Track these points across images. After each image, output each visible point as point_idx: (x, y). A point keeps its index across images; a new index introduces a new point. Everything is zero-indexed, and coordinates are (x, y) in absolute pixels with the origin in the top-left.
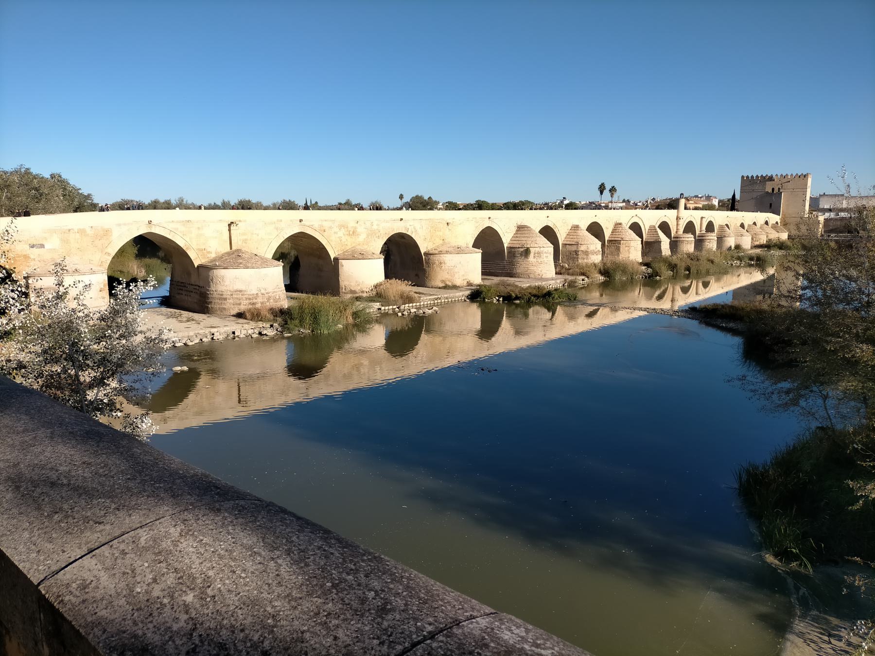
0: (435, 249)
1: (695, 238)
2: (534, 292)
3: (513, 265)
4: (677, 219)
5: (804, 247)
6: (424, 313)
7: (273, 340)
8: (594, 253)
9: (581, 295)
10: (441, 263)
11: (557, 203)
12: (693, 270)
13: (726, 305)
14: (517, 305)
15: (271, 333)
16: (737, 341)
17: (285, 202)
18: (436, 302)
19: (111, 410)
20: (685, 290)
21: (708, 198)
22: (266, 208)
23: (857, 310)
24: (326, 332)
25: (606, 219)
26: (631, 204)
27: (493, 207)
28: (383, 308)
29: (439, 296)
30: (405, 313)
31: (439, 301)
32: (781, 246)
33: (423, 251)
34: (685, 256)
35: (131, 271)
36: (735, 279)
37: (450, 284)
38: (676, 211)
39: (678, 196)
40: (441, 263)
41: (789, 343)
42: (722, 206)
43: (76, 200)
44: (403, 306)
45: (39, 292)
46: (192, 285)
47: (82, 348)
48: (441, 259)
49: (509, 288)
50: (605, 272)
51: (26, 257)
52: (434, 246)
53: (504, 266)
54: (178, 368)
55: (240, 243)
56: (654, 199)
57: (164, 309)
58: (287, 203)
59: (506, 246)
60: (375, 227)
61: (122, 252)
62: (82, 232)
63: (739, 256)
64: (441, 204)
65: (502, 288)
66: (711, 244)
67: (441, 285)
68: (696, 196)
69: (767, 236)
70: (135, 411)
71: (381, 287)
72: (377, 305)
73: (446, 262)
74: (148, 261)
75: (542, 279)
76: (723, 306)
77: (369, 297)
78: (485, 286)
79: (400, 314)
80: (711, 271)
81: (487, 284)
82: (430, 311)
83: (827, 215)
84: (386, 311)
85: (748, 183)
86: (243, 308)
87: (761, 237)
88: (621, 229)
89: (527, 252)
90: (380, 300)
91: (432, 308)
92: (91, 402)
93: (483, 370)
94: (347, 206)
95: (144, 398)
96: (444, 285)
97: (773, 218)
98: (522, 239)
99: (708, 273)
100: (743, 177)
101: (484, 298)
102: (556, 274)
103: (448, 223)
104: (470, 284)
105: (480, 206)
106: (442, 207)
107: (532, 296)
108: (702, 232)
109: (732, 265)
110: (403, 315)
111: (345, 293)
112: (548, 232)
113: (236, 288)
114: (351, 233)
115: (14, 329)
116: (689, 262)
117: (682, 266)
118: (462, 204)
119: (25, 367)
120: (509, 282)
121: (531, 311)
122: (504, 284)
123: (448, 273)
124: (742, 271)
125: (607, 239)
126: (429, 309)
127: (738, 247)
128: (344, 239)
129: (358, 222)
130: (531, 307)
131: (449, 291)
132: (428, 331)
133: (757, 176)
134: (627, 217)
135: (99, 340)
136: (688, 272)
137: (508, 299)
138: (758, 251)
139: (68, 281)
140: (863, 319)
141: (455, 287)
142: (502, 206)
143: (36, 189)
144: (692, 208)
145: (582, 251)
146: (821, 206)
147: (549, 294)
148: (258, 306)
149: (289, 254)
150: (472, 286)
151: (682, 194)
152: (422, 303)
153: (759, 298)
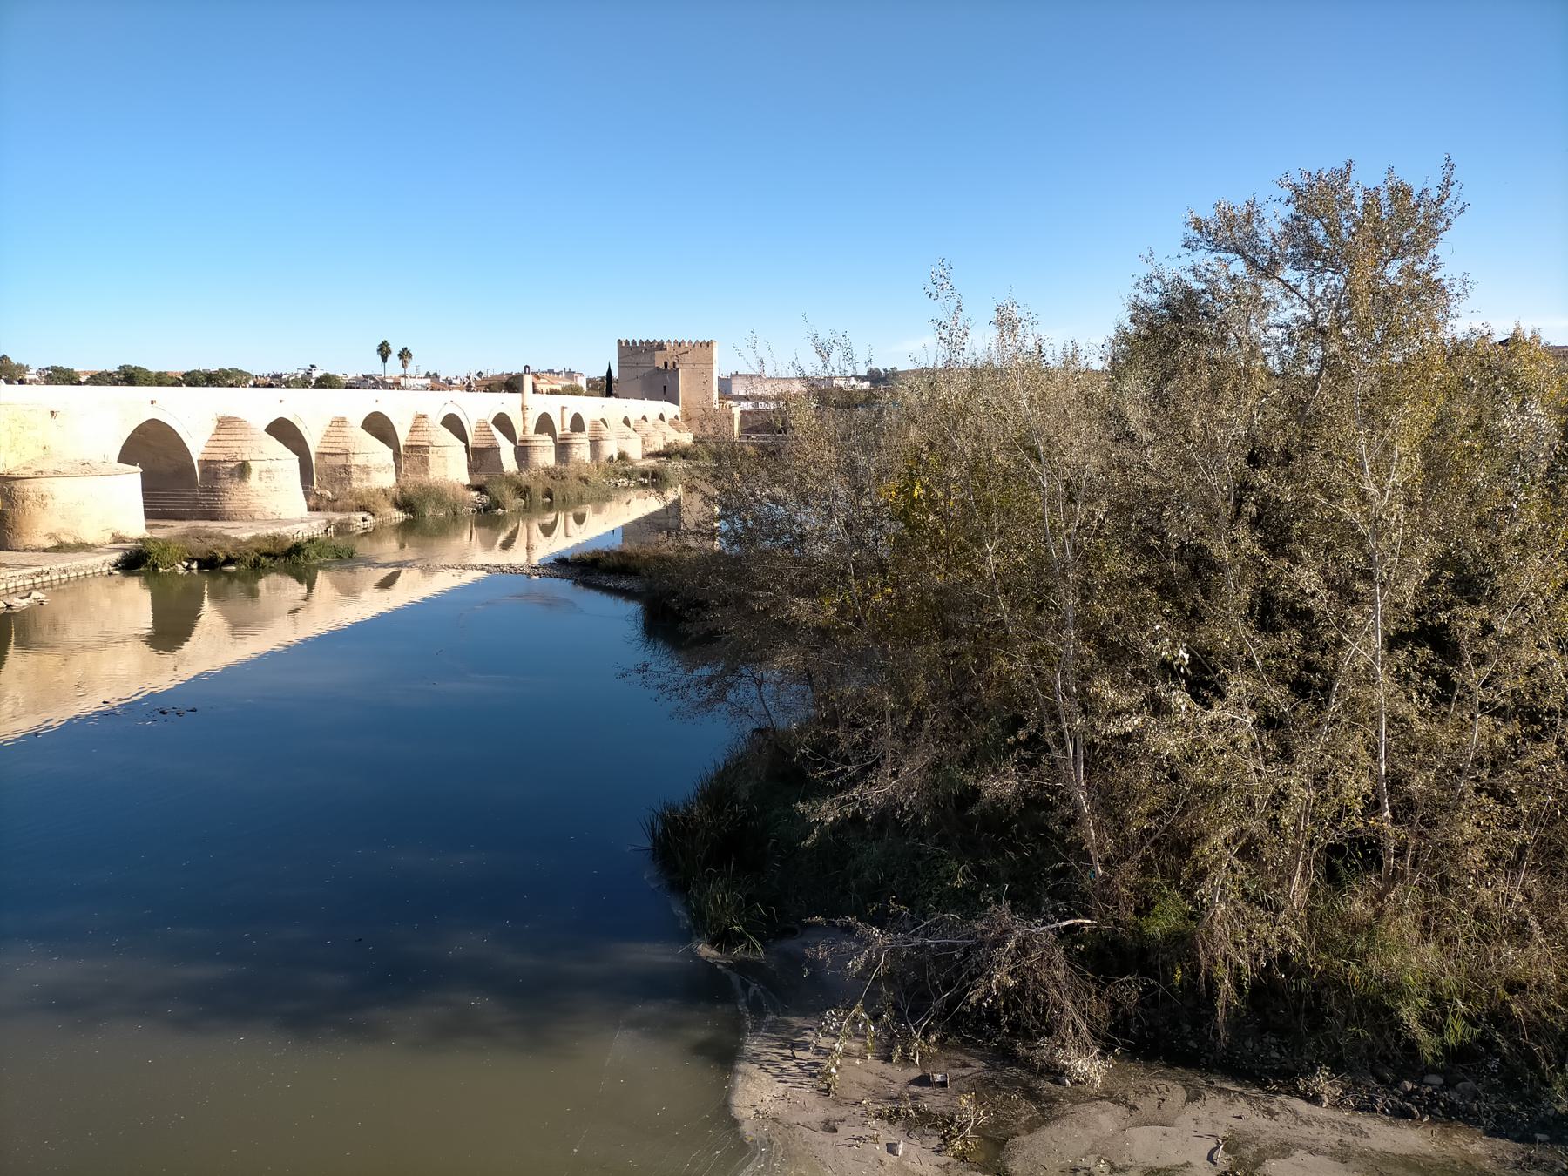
0: (25, 468)
1: (555, 441)
2: (266, 547)
3: (216, 496)
4: (522, 409)
5: (717, 457)
6: (9, 606)
8: (380, 469)
9: (363, 548)
11: (299, 376)
12: (557, 494)
13: (612, 551)
14: (231, 576)
16: (633, 608)
18: (38, 580)
20: (548, 530)
21: (570, 374)
25: (399, 408)
26: (441, 381)
27: (161, 380)
32: (684, 454)
34: (542, 471)
36: (623, 506)
37: (70, 540)
38: (519, 395)
39: (521, 370)
42: (592, 389)
49: (211, 543)
50: (404, 504)
53: (198, 500)
56: (480, 374)
59: (196, 457)
63: (625, 471)
65: (194, 543)
67: (48, 544)
68: (551, 372)
69: (665, 439)
75: (279, 521)
76: (607, 553)
78: (155, 541)
80: (586, 496)
81: (161, 536)
82: (25, 603)
83: (744, 404)
85: (630, 352)
87: (655, 439)
88: (426, 425)
89: (243, 470)
93: (163, 713)
96: (55, 544)
97: (671, 410)
98: (231, 444)
99: (581, 500)
100: (619, 342)
101: (155, 566)
102: (309, 510)
103: (52, 413)
104: (117, 539)
105: (130, 377)
106: (37, 378)
107: (261, 555)
108: (565, 432)
109: (617, 485)
112: (283, 431)
116: (549, 482)
117: (537, 489)
118: (86, 373)
120: (211, 530)
121: (262, 584)
122: (197, 535)
124: (632, 495)
125: (402, 443)
126: (21, 598)
127: (623, 456)
130: (261, 578)
132: (24, 644)
133: (641, 342)
134: (437, 405)
136: (548, 500)
137: (210, 564)
138: (653, 462)
141: (82, 547)
142: (181, 378)
144: (545, 391)
145: (357, 466)
146: (735, 392)
147: (297, 549)
150: (124, 542)
151: (527, 367)
153: (662, 536)
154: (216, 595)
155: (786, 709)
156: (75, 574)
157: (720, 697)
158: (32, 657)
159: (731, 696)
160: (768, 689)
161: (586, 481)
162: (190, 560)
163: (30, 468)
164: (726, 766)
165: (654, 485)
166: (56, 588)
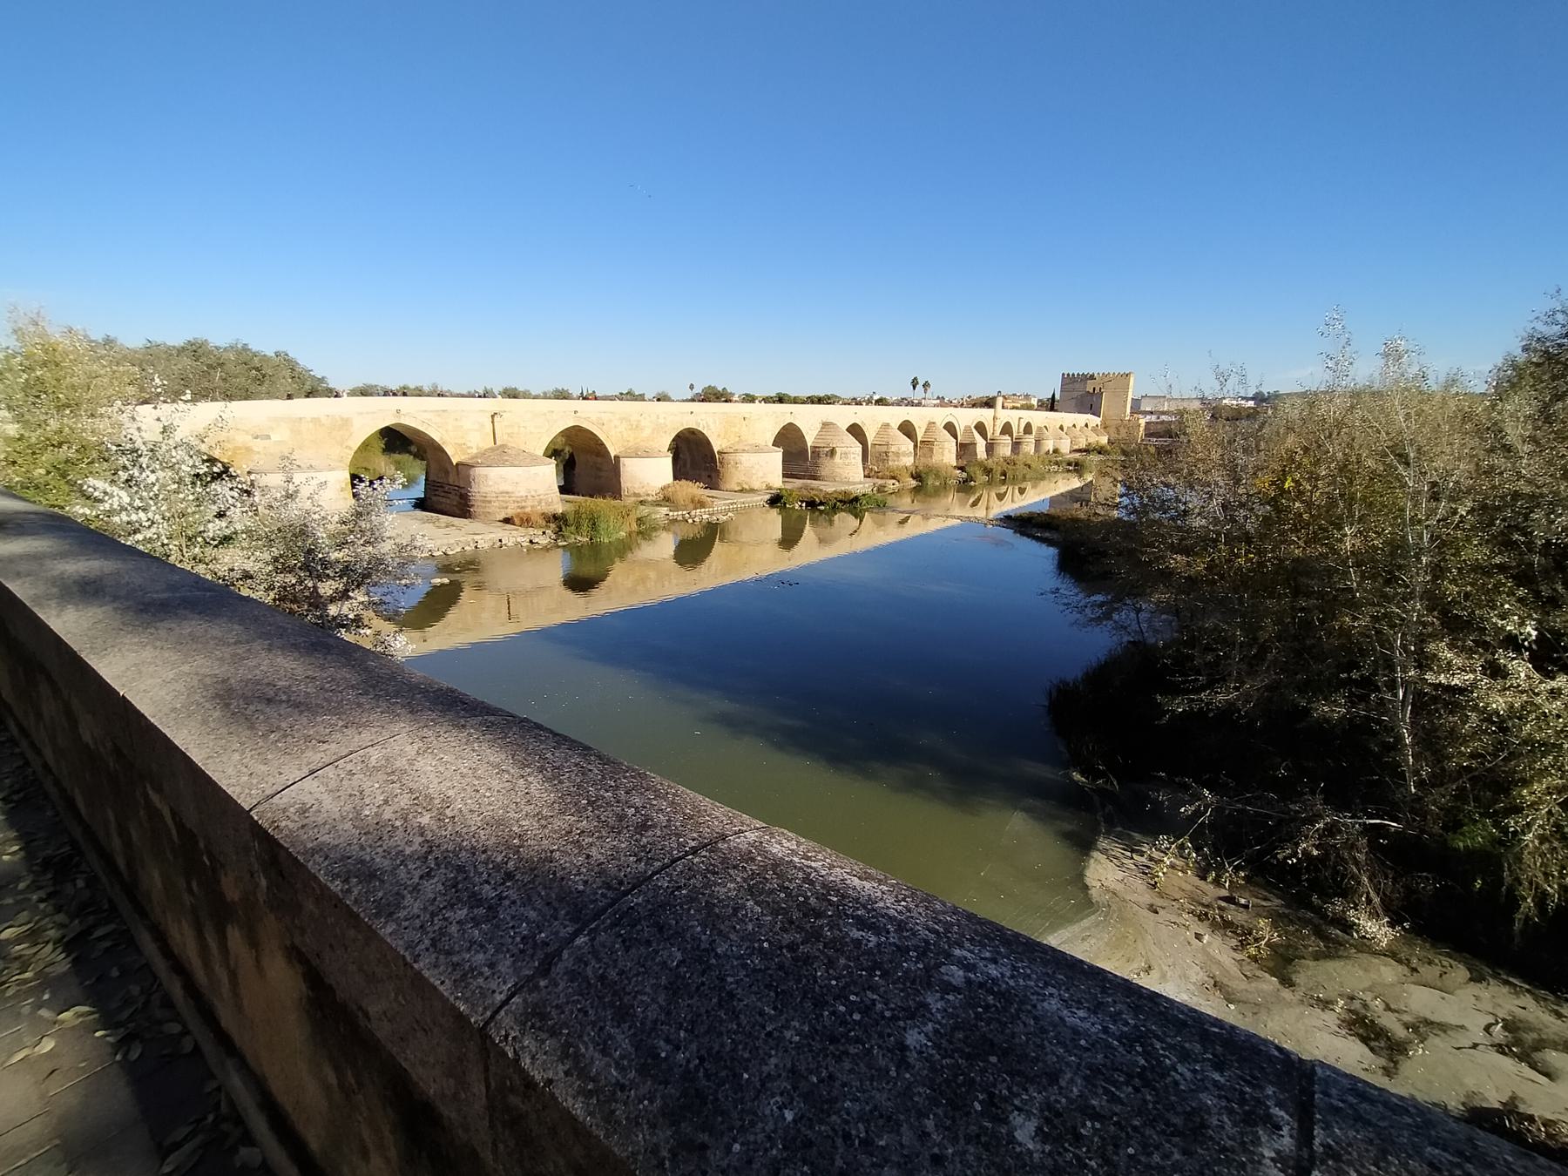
5: (1124, 453)
7: (546, 549)
8: (905, 454)
9: (891, 501)
14: (821, 512)
15: (543, 541)
17: (557, 391)
19: (358, 627)
20: (1001, 497)
21: (1027, 397)
22: (536, 397)
23: (1172, 518)
24: (606, 541)
25: (920, 417)
27: (795, 401)
28: (671, 514)
32: (1101, 451)
35: (378, 469)
36: (1052, 485)
37: (747, 487)
38: (992, 410)
41: (1104, 554)
43: (308, 383)
45: (265, 490)
47: (320, 556)
49: (814, 492)
50: (917, 476)
51: (249, 449)
54: (437, 581)
55: (505, 437)
56: (969, 397)
57: (419, 513)
58: (559, 391)
60: (662, 421)
61: (366, 445)
62: (316, 421)
65: (805, 492)
66: (1029, 447)
68: (1014, 395)
70: (387, 628)
72: (664, 510)
74: (397, 456)
75: (848, 483)
79: (690, 521)
82: (725, 518)
83: (1148, 417)
86: (510, 513)
89: (832, 452)
92: (334, 618)
94: (631, 396)
95: (397, 613)
97: (1094, 420)
99: (1024, 479)
100: (1063, 374)
101: (785, 504)
105: (781, 399)
112: (856, 431)
113: (501, 489)
115: (236, 533)
119: (251, 577)
121: (836, 517)
122: (806, 487)
124: (1059, 476)
125: (919, 439)
127: (1056, 451)
131: (747, 495)
134: (942, 416)
135: (340, 546)
137: (812, 504)
138: (1077, 455)
139: (298, 478)
140: (1179, 529)
141: (752, 491)
143: (257, 369)
146: (1142, 409)
147: (856, 499)
148: (528, 510)
149: (563, 450)
154: (814, 522)
155: (1156, 631)
157: (1107, 616)
159: (1115, 616)
160: (1143, 615)
161: (1029, 467)
162: (802, 502)
164: (1106, 662)
165: (1076, 471)
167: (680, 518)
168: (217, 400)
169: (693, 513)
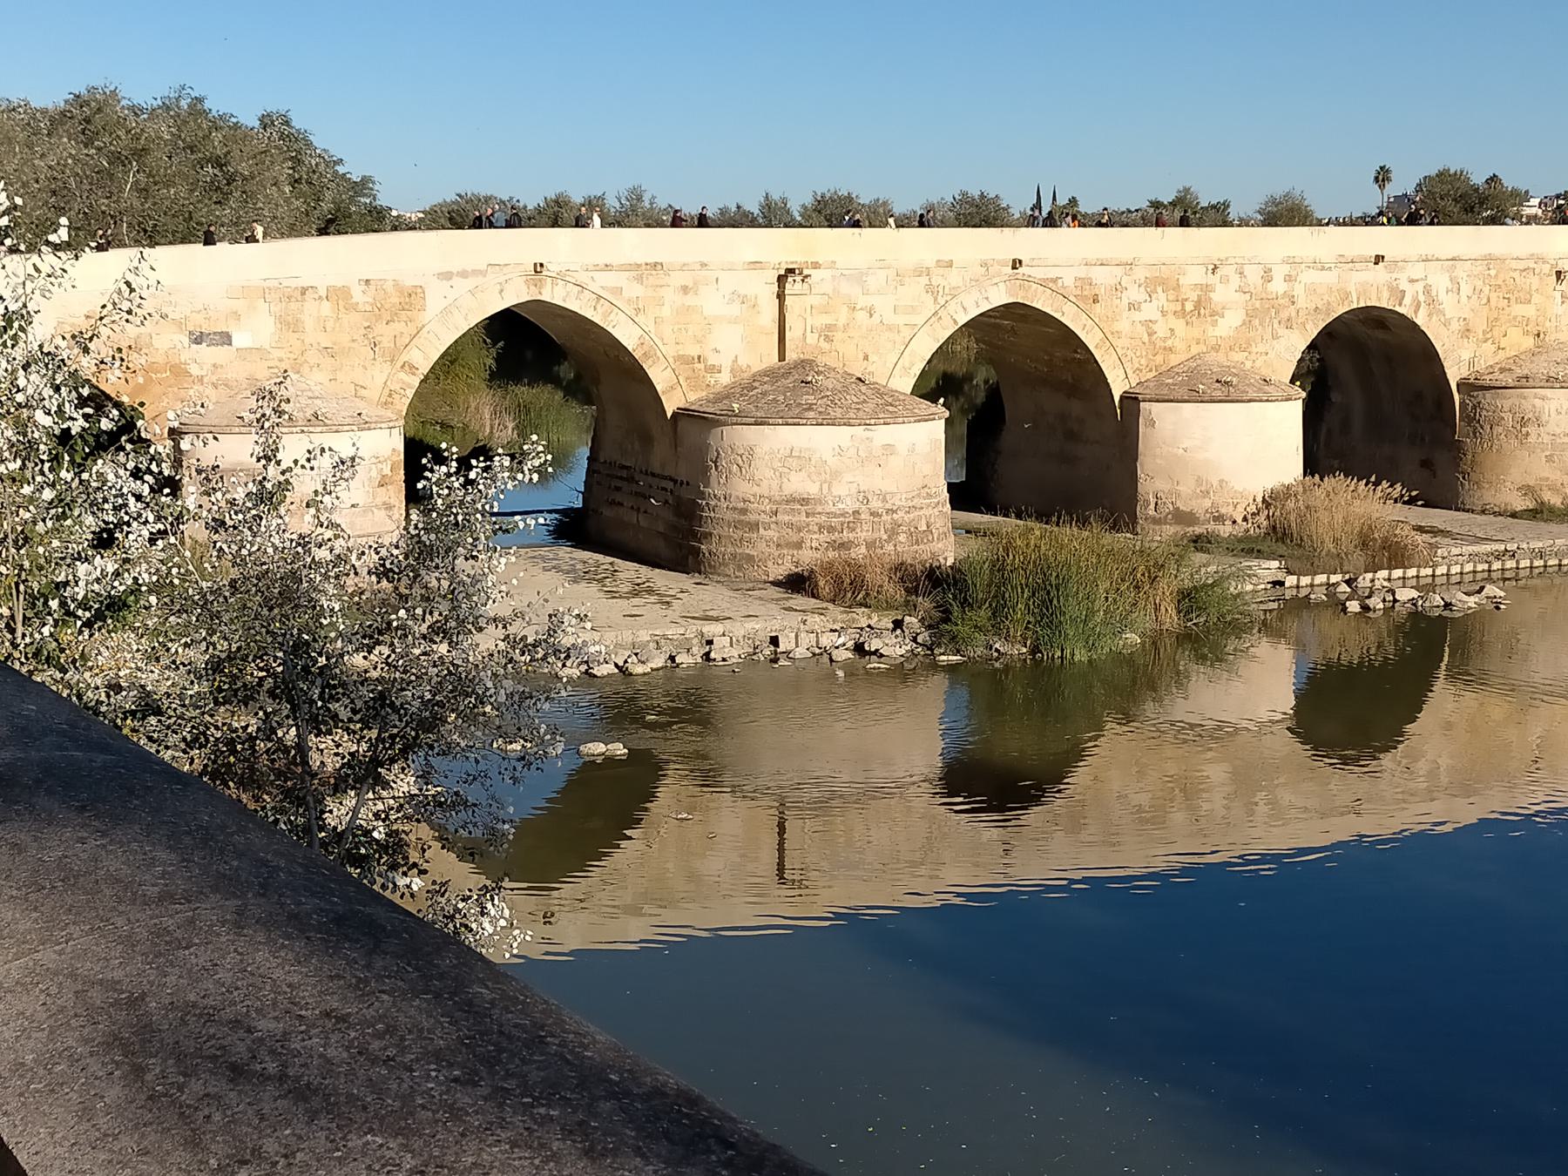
0: (1502, 370)
6: (1447, 605)
7: (901, 673)
10: (1523, 422)
15: (894, 648)
17: (965, 199)
18: (1496, 565)
19: (394, 867)
24: (1081, 656)
28: (1291, 581)
29: (1512, 547)
30: (1371, 602)
31: (1510, 564)
33: (1454, 376)
35: (474, 426)
40: (1523, 422)
43: (328, 195)
44: (1369, 576)
45: (210, 477)
46: (653, 475)
47: (322, 661)
48: (1526, 405)
51: (179, 371)
52: (1501, 355)
54: (597, 748)
55: (812, 339)
57: (568, 554)
61: (450, 360)
62: (338, 295)
64: (1534, 202)
67: (1520, 504)
70: (463, 876)
71: (1291, 504)
72: (1269, 569)
73: (1545, 418)
74: (523, 392)
77: (1240, 540)
79: (1353, 606)
82: (1472, 601)
84: (1303, 593)
86: (808, 558)
90: (1282, 549)
91: (1482, 588)
92: (338, 837)
95: (494, 836)
96: (1530, 504)
103: (1559, 273)
106: (1540, 212)
110: (1366, 608)
111: (1156, 521)
114: (1189, 306)
115: (135, 590)
119: (158, 712)
123: (1549, 459)
128: (1161, 330)
129: (1216, 267)
135: (370, 639)
139: (292, 448)
143: (219, 164)
148: (859, 553)
149: (968, 378)
152: (1441, 570)
156: (1557, 562)
158: (1470, 698)
163: (1510, 369)
166: (1521, 583)
167: (1320, 595)
168: (125, 246)
169: (1364, 580)
